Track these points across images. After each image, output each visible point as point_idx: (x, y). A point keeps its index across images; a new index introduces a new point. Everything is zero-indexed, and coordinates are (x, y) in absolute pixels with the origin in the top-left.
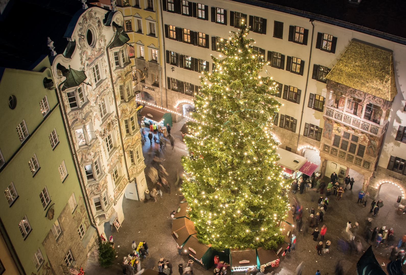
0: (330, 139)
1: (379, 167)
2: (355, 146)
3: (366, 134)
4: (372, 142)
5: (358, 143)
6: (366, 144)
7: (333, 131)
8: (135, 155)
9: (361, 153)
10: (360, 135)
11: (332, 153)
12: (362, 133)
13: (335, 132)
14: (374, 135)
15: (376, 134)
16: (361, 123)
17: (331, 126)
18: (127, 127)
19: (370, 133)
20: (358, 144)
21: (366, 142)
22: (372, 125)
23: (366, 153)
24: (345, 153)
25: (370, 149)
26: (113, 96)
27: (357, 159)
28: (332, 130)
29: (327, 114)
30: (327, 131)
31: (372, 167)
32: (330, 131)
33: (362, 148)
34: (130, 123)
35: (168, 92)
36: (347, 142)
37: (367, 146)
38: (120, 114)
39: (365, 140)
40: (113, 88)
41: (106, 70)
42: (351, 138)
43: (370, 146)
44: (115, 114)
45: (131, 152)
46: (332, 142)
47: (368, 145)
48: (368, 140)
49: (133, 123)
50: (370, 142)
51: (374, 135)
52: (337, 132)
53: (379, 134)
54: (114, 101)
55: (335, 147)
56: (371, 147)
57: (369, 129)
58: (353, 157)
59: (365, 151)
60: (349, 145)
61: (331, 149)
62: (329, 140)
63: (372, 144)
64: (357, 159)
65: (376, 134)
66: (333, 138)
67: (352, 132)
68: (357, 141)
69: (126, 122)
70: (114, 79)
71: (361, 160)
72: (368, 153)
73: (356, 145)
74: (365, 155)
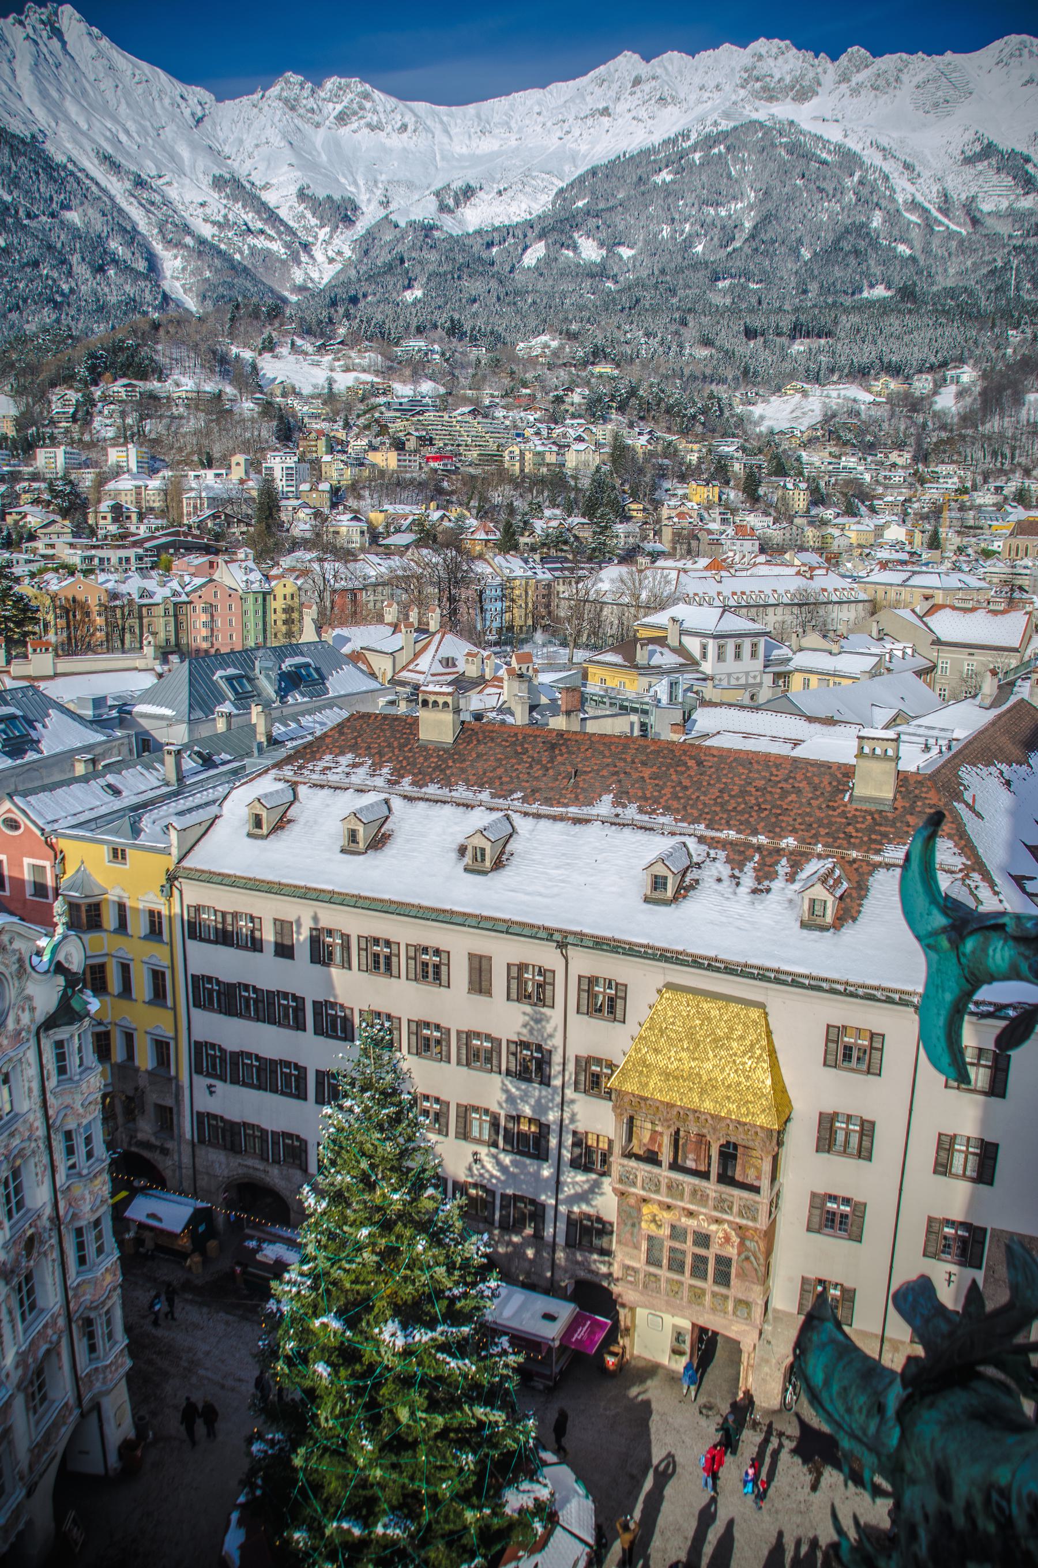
0: (637, 1247)
1: (775, 1310)
2: (704, 1260)
3: (729, 1222)
6: (732, 1251)
7: (643, 1225)
8: (100, 1330)
9: (723, 1278)
10: (714, 1227)
11: (645, 1286)
12: (717, 1221)
13: (647, 1227)
14: (750, 1224)
15: (754, 1219)
16: (712, 1195)
17: (635, 1214)
18: (81, 1246)
19: (738, 1220)
20: (710, 1254)
23: (737, 1276)
24: (681, 1283)
26: (46, 1160)
27: (714, 1295)
29: (621, 1181)
30: (628, 1228)
31: (758, 1312)
33: (723, 1263)
34: (90, 1237)
35: (198, 1152)
36: (683, 1252)
37: (735, 1257)
38: (62, 1212)
39: (727, 1239)
40: (49, 1138)
41: (30, 1090)
42: (690, 1239)
44: (48, 1211)
45: (89, 1322)
46: (643, 1257)
48: (735, 1239)
49: (99, 1237)
50: (742, 1243)
51: (750, 1224)
52: (653, 1226)
53: (762, 1223)
54: (49, 1172)
55: (652, 1269)
56: (747, 1258)
57: (735, 1209)
58: (703, 1292)
59: (733, 1271)
60: (689, 1261)
61: (642, 1276)
63: (748, 1249)
64: (714, 1295)
65: (754, 1219)
66: (644, 1246)
67: (691, 1223)
68: (707, 1246)
69: (79, 1232)
70: (51, 1112)
71: (726, 1298)
72: (742, 1275)
74: (734, 1280)
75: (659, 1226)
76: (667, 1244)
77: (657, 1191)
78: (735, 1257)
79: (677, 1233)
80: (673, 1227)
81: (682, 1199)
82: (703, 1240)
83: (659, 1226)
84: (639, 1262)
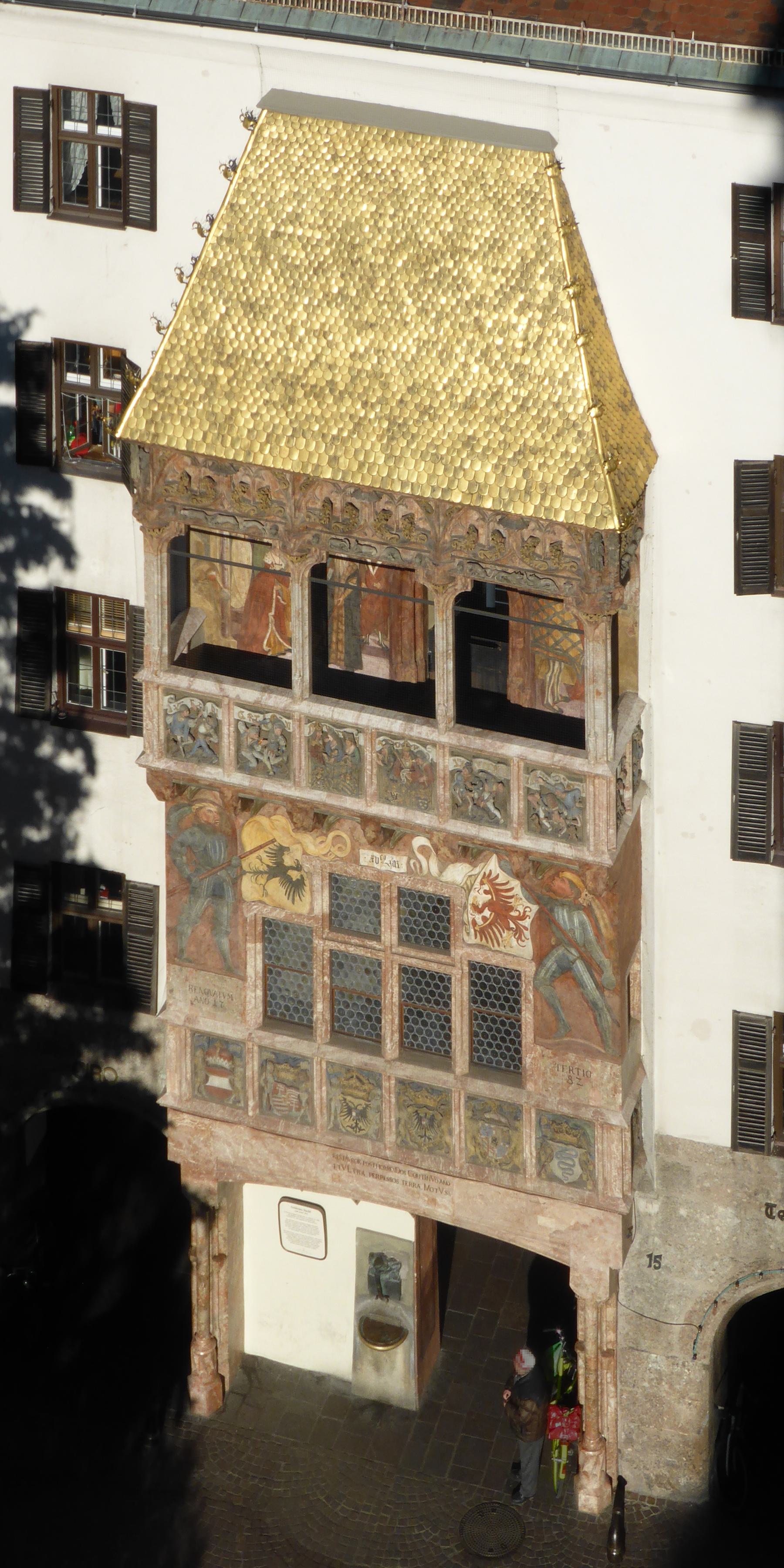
0: (232, 968)
4: (562, 915)
5: (459, 952)
6: (516, 951)
10: (458, 873)
12: (469, 851)
13: (262, 898)
14: (564, 850)
15: (575, 835)
16: (448, 764)
21: (518, 933)
22: (530, 768)
25: (560, 989)
28: (236, 882)
32: (217, 893)
33: (495, 989)
36: (373, 970)
37: (529, 970)
39: (500, 909)
43: (551, 963)
47: (540, 958)
48: (525, 907)
51: (564, 850)
60: (392, 994)
62: (229, 984)
65: (575, 835)
67: (387, 865)
73: (444, 981)
75: (296, 887)
76: (322, 945)
77: (283, 771)
78: (529, 970)
79: (352, 903)
80: (336, 883)
81: (357, 790)
82: (429, 919)
83: (296, 887)
84: (241, 1018)
